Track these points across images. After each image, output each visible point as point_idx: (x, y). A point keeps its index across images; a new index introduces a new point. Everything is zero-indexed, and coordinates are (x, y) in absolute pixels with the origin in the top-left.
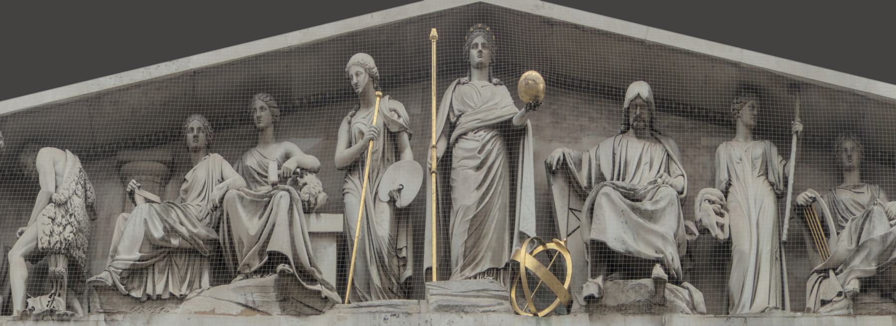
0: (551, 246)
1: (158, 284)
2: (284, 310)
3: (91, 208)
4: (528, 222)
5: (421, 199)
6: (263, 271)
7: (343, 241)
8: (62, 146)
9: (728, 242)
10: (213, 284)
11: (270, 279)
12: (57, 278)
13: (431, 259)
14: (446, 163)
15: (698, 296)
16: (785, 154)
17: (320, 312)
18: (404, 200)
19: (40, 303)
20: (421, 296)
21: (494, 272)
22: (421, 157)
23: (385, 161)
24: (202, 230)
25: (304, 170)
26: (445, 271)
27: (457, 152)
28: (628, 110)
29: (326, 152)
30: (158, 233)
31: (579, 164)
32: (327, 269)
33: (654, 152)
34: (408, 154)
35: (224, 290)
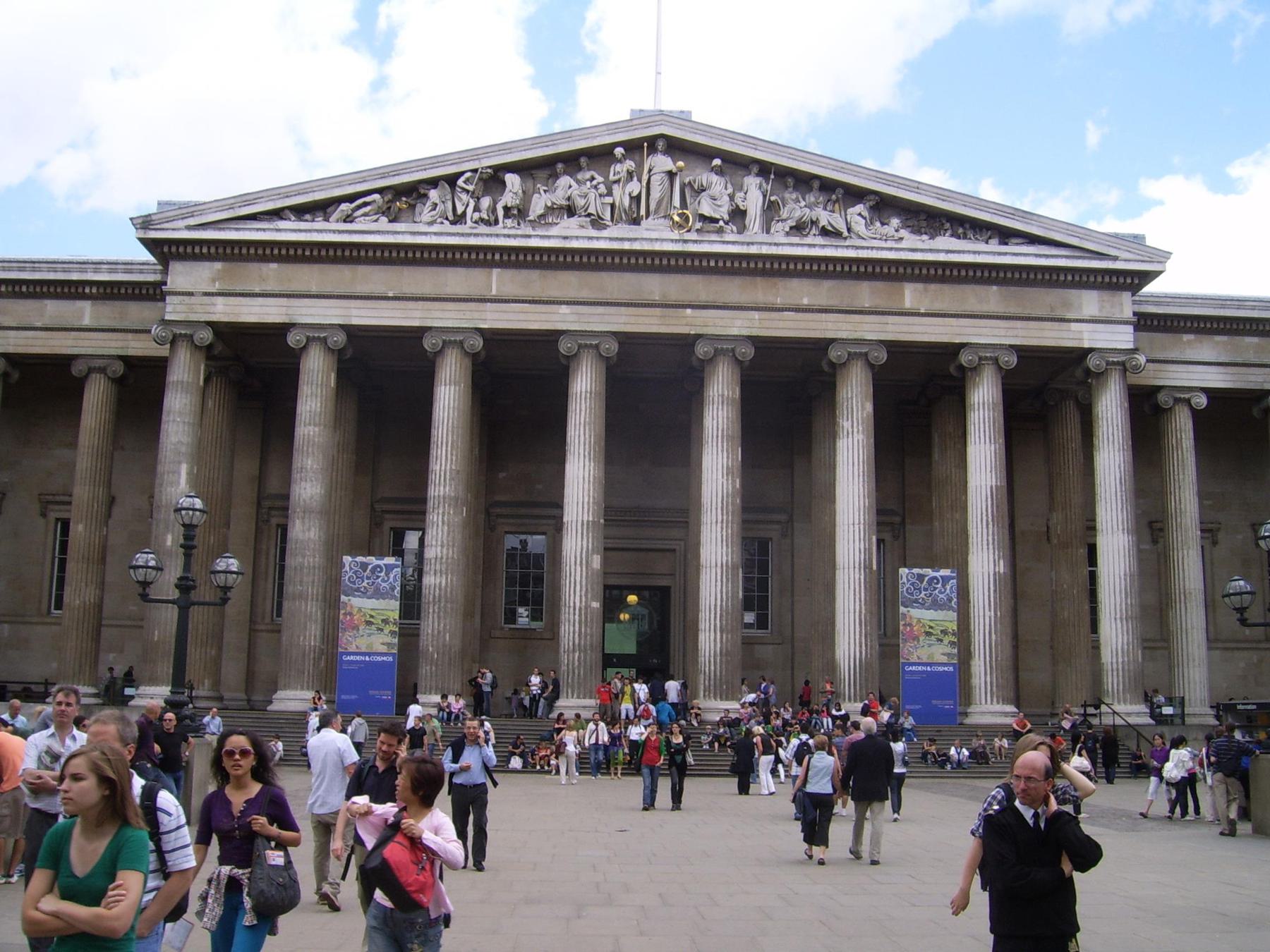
0: (685, 211)
2: (593, 228)
3: (524, 192)
5: (640, 193)
6: (586, 216)
8: (513, 172)
9: (746, 211)
11: (588, 219)
12: (514, 215)
13: (643, 212)
15: (735, 228)
16: (768, 184)
17: (605, 229)
18: (635, 194)
19: (509, 222)
20: (639, 224)
21: (665, 217)
22: (640, 180)
24: (564, 203)
25: (599, 183)
26: (648, 216)
27: (652, 178)
28: (713, 168)
29: (607, 177)
31: (695, 182)
32: (608, 215)
34: (635, 179)
35: (572, 219)
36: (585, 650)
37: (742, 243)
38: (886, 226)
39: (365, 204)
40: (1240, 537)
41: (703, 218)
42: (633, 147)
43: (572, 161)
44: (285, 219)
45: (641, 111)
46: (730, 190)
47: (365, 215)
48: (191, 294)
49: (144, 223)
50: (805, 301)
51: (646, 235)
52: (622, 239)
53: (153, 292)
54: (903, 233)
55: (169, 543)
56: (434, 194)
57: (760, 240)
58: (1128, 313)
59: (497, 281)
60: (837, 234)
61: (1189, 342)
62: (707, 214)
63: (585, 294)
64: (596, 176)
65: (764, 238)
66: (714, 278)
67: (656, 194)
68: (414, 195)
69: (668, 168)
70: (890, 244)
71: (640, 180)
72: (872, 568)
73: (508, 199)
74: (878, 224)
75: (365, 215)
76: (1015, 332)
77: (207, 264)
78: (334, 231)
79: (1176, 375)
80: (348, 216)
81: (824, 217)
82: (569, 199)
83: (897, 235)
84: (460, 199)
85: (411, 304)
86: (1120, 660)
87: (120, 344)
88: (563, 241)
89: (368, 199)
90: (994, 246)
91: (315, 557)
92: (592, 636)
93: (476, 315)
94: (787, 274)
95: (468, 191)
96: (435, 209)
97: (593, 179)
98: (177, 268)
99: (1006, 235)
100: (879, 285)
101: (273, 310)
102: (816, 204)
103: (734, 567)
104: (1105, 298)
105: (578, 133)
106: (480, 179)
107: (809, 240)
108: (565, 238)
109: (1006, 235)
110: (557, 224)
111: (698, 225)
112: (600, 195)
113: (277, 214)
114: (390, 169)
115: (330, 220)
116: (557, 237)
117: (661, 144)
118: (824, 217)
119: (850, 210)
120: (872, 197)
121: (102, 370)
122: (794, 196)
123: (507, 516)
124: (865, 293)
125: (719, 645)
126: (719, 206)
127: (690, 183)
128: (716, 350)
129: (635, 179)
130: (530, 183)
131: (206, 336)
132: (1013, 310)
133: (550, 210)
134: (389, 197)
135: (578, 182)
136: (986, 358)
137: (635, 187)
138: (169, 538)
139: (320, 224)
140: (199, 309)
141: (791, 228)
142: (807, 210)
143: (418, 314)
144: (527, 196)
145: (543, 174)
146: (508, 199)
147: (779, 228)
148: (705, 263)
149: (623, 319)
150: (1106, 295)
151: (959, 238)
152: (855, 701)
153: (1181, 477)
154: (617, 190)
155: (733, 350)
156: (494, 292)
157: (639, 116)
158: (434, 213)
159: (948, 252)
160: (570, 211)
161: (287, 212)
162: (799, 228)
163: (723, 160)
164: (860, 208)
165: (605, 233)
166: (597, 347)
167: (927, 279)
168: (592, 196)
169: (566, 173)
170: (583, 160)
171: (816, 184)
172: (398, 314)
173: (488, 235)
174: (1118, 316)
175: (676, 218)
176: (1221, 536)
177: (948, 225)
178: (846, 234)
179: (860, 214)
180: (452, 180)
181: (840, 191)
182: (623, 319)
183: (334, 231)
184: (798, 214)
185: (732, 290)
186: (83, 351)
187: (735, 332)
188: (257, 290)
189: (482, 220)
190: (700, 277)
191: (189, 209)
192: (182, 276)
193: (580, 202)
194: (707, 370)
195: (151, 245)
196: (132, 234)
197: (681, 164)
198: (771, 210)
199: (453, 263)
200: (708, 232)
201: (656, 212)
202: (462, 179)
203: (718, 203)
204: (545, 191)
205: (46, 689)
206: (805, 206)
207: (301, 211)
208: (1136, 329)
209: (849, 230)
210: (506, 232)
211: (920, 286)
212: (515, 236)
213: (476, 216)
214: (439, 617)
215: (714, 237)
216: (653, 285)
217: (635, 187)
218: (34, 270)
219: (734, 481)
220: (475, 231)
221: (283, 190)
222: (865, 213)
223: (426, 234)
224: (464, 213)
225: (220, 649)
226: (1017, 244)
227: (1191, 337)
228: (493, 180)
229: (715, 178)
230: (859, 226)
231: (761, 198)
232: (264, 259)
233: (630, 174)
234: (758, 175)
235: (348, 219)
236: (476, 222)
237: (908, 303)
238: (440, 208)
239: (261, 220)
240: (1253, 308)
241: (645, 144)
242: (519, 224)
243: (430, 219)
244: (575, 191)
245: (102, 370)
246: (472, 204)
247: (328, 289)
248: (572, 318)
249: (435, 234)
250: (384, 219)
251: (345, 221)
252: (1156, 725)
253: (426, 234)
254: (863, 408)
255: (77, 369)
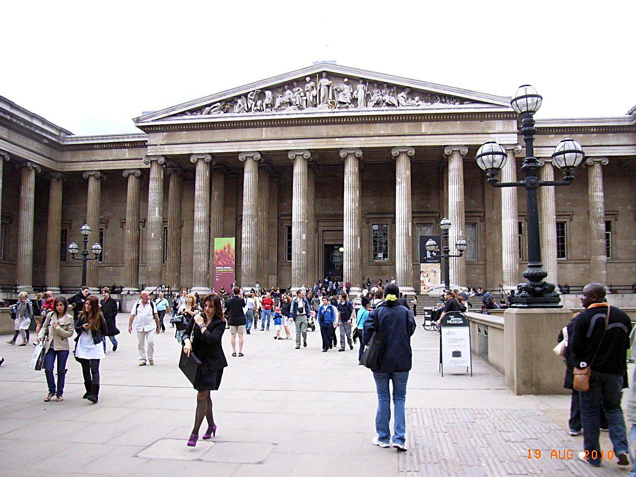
1: (282, 108)
3: (273, 98)
4: (331, 97)
5: (316, 96)
7: (306, 100)
10: (290, 106)
13: (318, 102)
14: (320, 90)
15: (353, 106)
19: (267, 109)
21: (326, 103)
22: (316, 90)
23: (312, 90)
24: (288, 101)
29: (304, 89)
30: (282, 102)
33: (348, 87)
34: (315, 89)
36: (300, 270)
37: (355, 112)
38: (413, 100)
39: (215, 107)
40: (582, 217)
41: (340, 103)
42: (313, 77)
43: (291, 84)
44: (186, 115)
45: (317, 62)
46: (352, 91)
47: (215, 111)
48: (156, 145)
49: (137, 120)
50: (382, 132)
51: (319, 111)
52: (309, 113)
53: (143, 145)
54: (420, 103)
55: (153, 236)
56: (239, 101)
57: (363, 110)
58: (515, 129)
59: (265, 133)
60: (393, 105)
61: (552, 138)
62: (342, 101)
63: (298, 136)
64: (300, 89)
65: (366, 109)
66: (347, 125)
67: (322, 95)
68: (233, 102)
69: (327, 84)
70: (414, 108)
71: (316, 90)
72: (408, 236)
73: (267, 101)
74: (410, 100)
75: (215, 111)
76: (467, 140)
77: (161, 134)
78: (203, 118)
79: (546, 152)
80: (209, 112)
81: (387, 98)
82: (290, 99)
83: (417, 104)
84: (249, 102)
85: (234, 143)
86: (509, 269)
87: (139, 164)
88: (286, 115)
89: (215, 105)
90: (457, 105)
91: (203, 239)
92: (302, 264)
93: (257, 146)
94: (375, 122)
95: (252, 99)
96: (240, 107)
97: (299, 90)
98: (151, 135)
99: (462, 100)
100: (411, 123)
101: (185, 149)
102: (386, 93)
103: (356, 237)
104: (506, 123)
105: (290, 74)
106: (256, 94)
107: (381, 108)
108: (288, 114)
109: (462, 100)
110: (285, 109)
111: (338, 106)
112: (301, 97)
113: (183, 113)
114: (223, 93)
115: (204, 113)
116: (285, 114)
117: (324, 75)
118: (387, 98)
119: (398, 95)
120: (408, 89)
121: (133, 174)
122: (377, 91)
123: (286, 220)
124: (406, 128)
125: (350, 266)
126: (346, 98)
127: (336, 89)
128: (348, 153)
129: (315, 89)
130: (276, 94)
131: (162, 160)
132: (466, 131)
133: (282, 104)
134: (223, 104)
135: (294, 92)
136: (455, 151)
137: (314, 92)
138: (153, 234)
139: (199, 116)
140: (159, 150)
141: (375, 104)
142: (381, 96)
143: (237, 147)
144: (274, 99)
145: (281, 90)
146: (267, 101)
147: (371, 104)
148: (342, 120)
149: (312, 144)
150: (505, 122)
151: (443, 103)
152: (404, 286)
153: (547, 194)
154: (308, 93)
155: (354, 153)
156: (264, 137)
157: (317, 64)
158: (240, 108)
159: (437, 109)
160: (291, 104)
161: (187, 112)
162: (378, 104)
163: (348, 78)
164: (403, 94)
165: (303, 111)
166: (302, 155)
167: (431, 121)
168: (298, 97)
169: (289, 89)
170: (295, 84)
171: (385, 85)
172: (230, 147)
173: (259, 116)
174: (511, 131)
175: (330, 104)
176: (574, 217)
177: (439, 98)
178: (397, 104)
179: (402, 96)
180: (246, 95)
181: (395, 87)
182: (312, 144)
183: (203, 118)
184: (377, 98)
185: (354, 130)
186: (126, 168)
187: (354, 146)
188: (179, 142)
189: (258, 110)
190: (341, 125)
191: (153, 114)
192: (153, 139)
193: (293, 100)
194: (346, 161)
195: (141, 128)
196: (133, 124)
197: (331, 82)
198: (367, 97)
199: (249, 127)
200: (343, 108)
201: (323, 101)
202: (250, 94)
203: (346, 96)
204: (281, 97)
205: (121, 289)
206: (381, 95)
207: (192, 111)
208: (518, 134)
209: (398, 103)
210: (266, 114)
211: (428, 123)
212: (269, 115)
213: (255, 108)
214: (247, 259)
215: (345, 110)
216: (323, 130)
217: (314, 92)
218: (107, 139)
219: (355, 204)
220: (255, 114)
221: (185, 104)
222: (405, 96)
223: (236, 117)
224: (251, 107)
225: (179, 272)
226: (467, 104)
227: (553, 136)
228: (261, 94)
229: (345, 86)
230: (402, 101)
231: (364, 92)
232: (181, 130)
233: (313, 87)
234: (363, 84)
235: (209, 113)
236: (255, 111)
237: (423, 131)
238: (242, 106)
239: (178, 116)
240: (579, 122)
241: (317, 75)
242: (272, 110)
243: (238, 111)
244: (292, 96)
245: (133, 174)
246: (254, 104)
247: (203, 140)
248: (294, 145)
249: (240, 116)
250: (222, 112)
251: (208, 114)
252: (611, 293)
253: (236, 117)
254: (406, 173)
255: (125, 174)
